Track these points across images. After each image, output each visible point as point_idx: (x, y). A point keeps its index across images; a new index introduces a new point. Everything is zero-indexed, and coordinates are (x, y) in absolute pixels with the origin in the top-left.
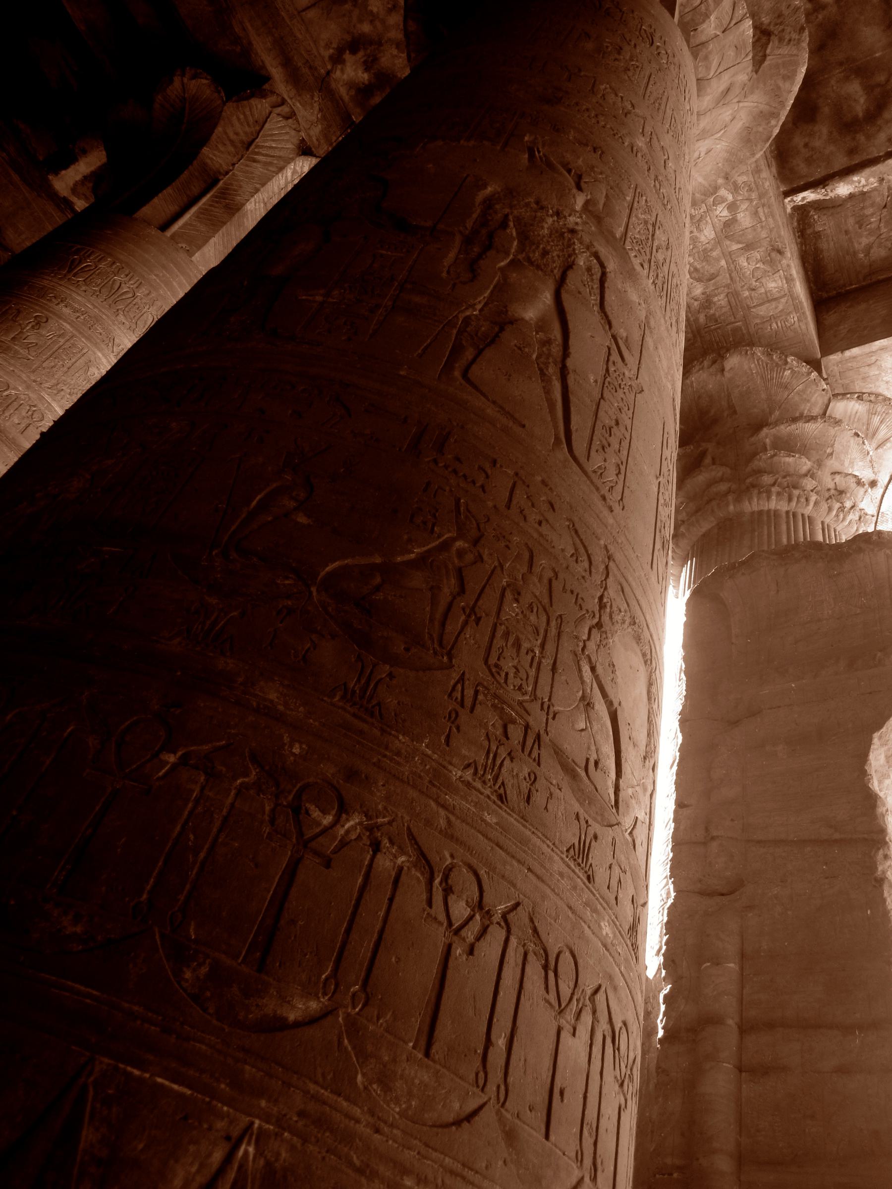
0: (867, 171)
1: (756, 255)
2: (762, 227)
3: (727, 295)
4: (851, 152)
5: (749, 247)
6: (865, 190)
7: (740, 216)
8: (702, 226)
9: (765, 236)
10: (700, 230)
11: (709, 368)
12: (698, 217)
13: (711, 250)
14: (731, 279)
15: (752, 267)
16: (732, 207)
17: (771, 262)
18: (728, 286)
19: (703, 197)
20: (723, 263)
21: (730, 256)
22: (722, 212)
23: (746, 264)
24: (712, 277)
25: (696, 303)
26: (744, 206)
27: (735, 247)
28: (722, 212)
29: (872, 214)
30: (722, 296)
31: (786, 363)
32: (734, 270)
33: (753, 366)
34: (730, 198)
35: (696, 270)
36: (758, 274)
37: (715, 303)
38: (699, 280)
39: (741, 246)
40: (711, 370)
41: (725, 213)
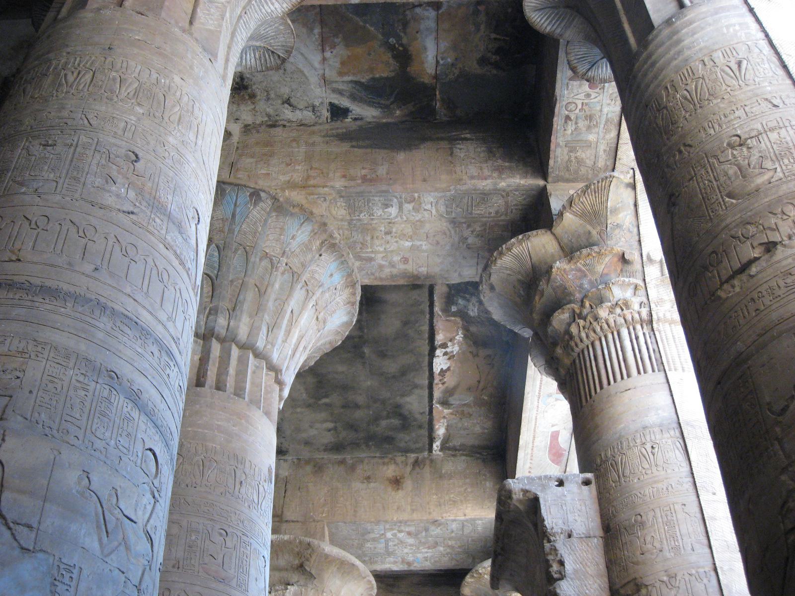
0: (435, 422)
4: (420, 427)
5: (427, 530)
6: (446, 424)
7: (407, 530)
10: (407, 543)
16: (400, 531)
22: (401, 535)
26: (403, 528)
27: (424, 534)
29: (463, 424)
31: (481, 574)
34: (395, 531)
41: (403, 534)
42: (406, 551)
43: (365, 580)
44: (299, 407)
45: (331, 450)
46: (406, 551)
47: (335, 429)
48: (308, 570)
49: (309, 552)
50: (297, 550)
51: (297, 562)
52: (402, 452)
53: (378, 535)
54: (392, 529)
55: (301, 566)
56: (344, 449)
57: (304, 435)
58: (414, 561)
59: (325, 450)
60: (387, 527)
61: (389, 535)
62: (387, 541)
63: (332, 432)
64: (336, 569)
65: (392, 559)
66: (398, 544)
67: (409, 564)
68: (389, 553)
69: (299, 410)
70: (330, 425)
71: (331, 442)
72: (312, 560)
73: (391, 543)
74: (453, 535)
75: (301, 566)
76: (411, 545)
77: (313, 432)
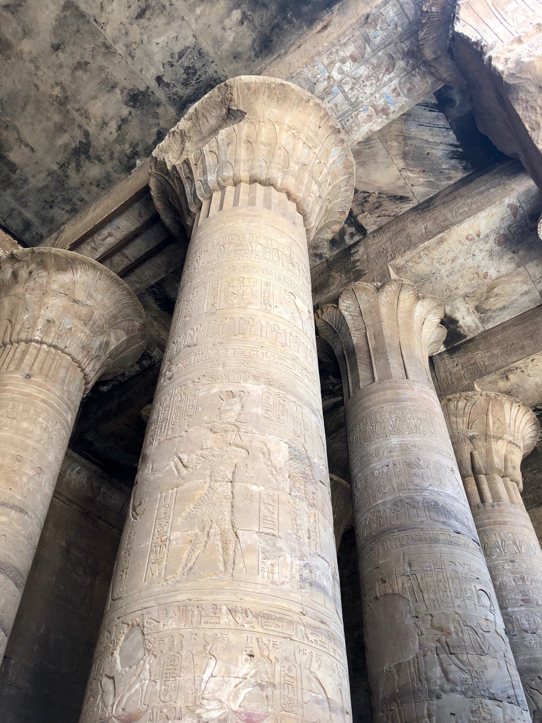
1: (371, 32)
2: (353, 36)
3: (402, 42)
5: (367, 40)
7: (348, 54)
8: (358, 76)
9: (358, 32)
11: (435, 67)
12: (353, 80)
13: (372, 64)
14: (390, 44)
15: (381, 32)
16: (343, 61)
17: (375, 20)
18: (395, 45)
19: (322, 110)
20: (380, 54)
21: (375, 52)
23: (379, 38)
24: (391, 57)
25: (411, 62)
26: (341, 53)
27: (368, 49)
28: (348, 66)
30: (404, 45)
31: (427, 11)
32: (384, 45)
33: (431, 37)
34: (338, 64)
35: (387, 70)
36: (385, 26)
37: (409, 49)
38: (394, 65)
39: (367, 46)
40: (437, 66)
41: (348, 64)
42: (368, 90)
43: (311, 104)
44: (195, 6)
45: (261, 51)
46: (368, 90)
47: (245, 16)
48: (235, 108)
49: (229, 92)
50: (220, 99)
51: (225, 111)
52: (324, 9)
53: (326, 82)
54: (332, 63)
55: (229, 110)
56: (271, 41)
57: (226, 46)
58: (386, 103)
59: (257, 56)
60: (326, 62)
61: (336, 76)
62: (340, 84)
63: (245, 23)
64: (266, 98)
65: (363, 116)
66: (354, 84)
67: (385, 111)
68: (355, 105)
69: (198, 11)
70: (237, 14)
71: (255, 40)
72: (235, 97)
73: (347, 88)
74: (400, 29)
75: (229, 110)
76: (368, 78)
77: (230, 36)
